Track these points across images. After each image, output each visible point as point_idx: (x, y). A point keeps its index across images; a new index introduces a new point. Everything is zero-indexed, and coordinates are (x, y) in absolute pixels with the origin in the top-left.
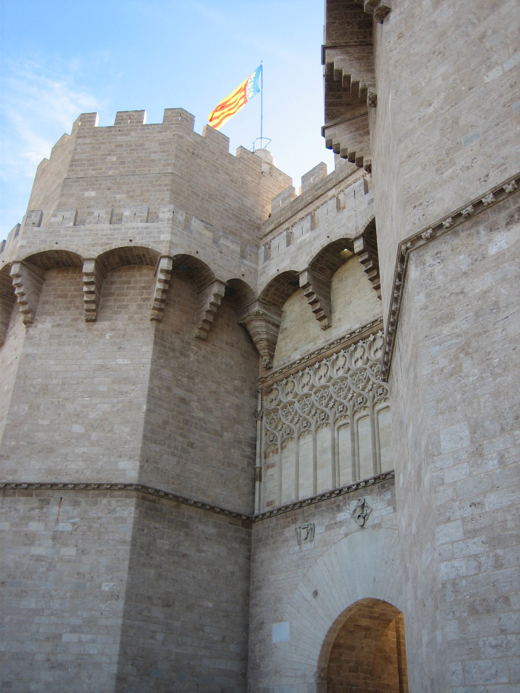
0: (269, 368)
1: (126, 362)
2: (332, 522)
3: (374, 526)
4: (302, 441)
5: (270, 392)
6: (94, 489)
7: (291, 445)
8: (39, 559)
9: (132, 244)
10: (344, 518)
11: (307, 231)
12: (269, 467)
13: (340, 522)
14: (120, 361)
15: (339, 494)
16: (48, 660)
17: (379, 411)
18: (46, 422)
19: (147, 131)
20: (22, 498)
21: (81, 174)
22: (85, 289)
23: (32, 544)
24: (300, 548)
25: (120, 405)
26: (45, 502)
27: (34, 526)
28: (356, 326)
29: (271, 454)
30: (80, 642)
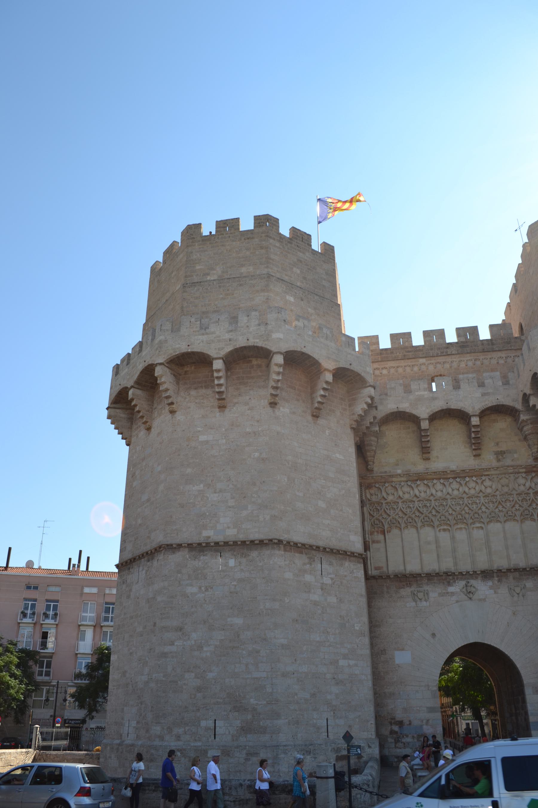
0: (372, 471)
1: (341, 457)
2: (444, 591)
3: (480, 600)
4: (406, 532)
5: (370, 488)
6: (340, 554)
7: (396, 531)
8: (316, 603)
9: (351, 368)
10: (454, 591)
11: (425, 390)
12: (373, 542)
13: (452, 593)
14: (338, 455)
15: (450, 575)
16: (334, 678)
17: (473, 528)
18: (301, 494)
19: (316, 256)
20: (297, 555)
21: (278, 275)
22: (322, 392)
23: (309, 592)
24: (416, 604)
25: (344, 491)
26: (311, 560)
27: (308, 578)
28: (454, 467)
29: (376, 533)
30: (349, 665)
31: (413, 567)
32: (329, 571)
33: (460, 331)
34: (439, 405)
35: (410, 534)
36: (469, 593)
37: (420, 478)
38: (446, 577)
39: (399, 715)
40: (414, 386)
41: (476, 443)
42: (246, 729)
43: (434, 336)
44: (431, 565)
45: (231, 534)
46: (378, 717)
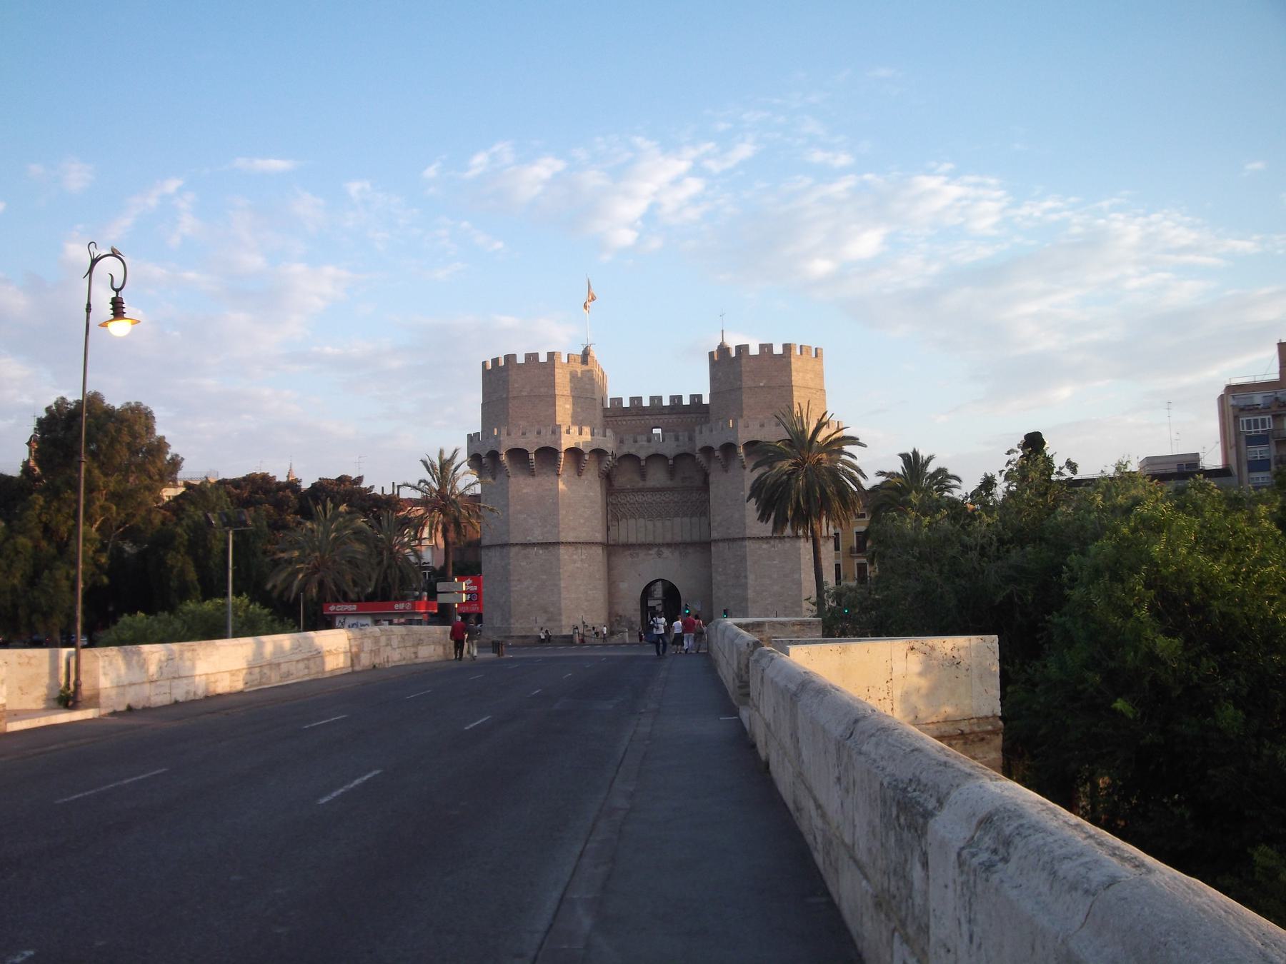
31: (632, 540)
32: (584, 553)
33: (672, 398)
34: (652, 451)
35: (632, 522)
36: (659, 554)
37: (640, 490)
38: (648, 546)
39: (621, 612)
40: (639, 438)
41: (672, 472)
42: (548, 620)
43: (656, 400)
44: (642, 538)
45: (540, 539)
46: (610, 614)
